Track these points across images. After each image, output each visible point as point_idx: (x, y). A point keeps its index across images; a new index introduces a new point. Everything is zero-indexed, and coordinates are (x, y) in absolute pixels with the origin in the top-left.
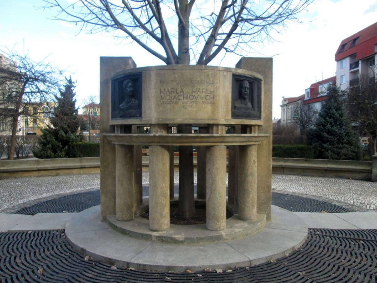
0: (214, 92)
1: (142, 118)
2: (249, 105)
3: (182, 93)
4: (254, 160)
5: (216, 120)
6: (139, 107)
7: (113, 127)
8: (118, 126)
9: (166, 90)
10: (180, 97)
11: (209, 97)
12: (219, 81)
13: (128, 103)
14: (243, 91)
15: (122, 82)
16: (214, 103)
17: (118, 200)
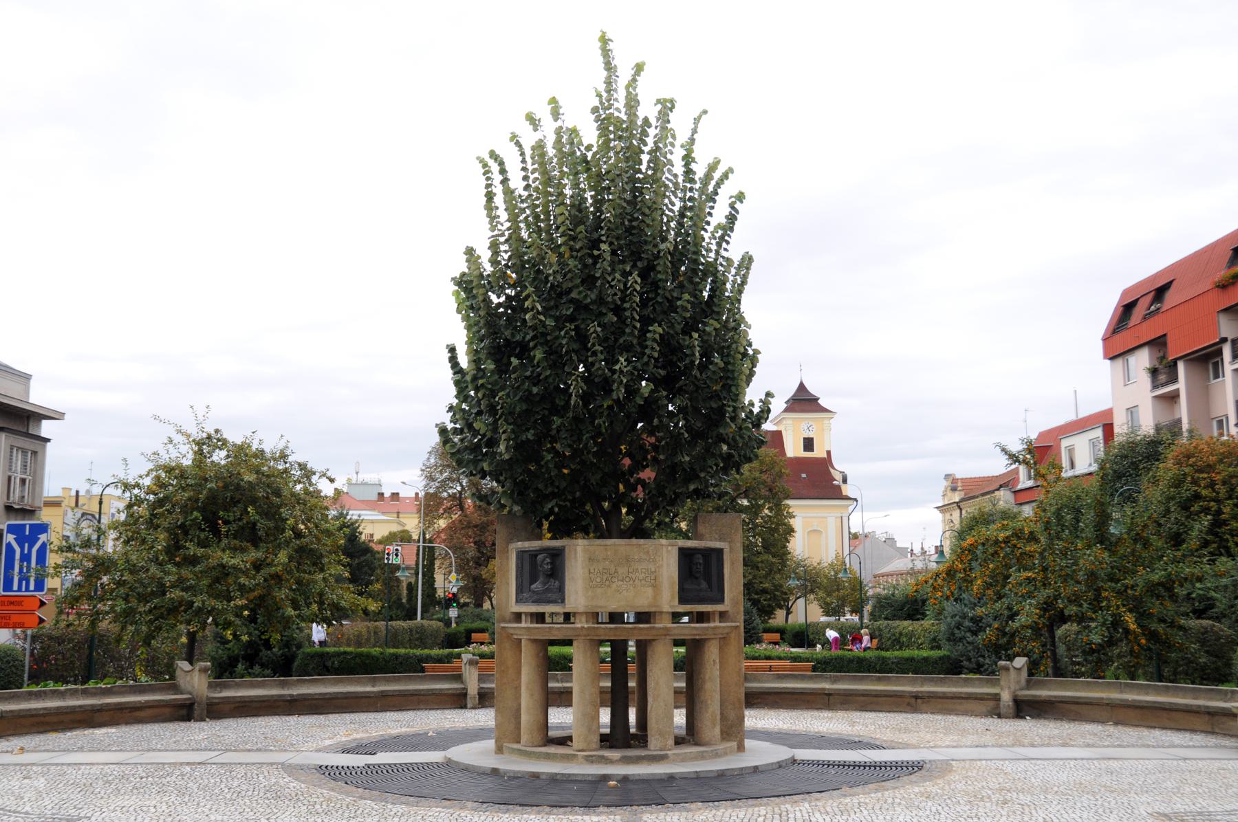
2: (704, 585)
6: (561, 589)
7: (518, 617)
8: (526, 614)
13: (545, 584)
15: (536, 556)
16: (655, 586)
17: (524, 718)
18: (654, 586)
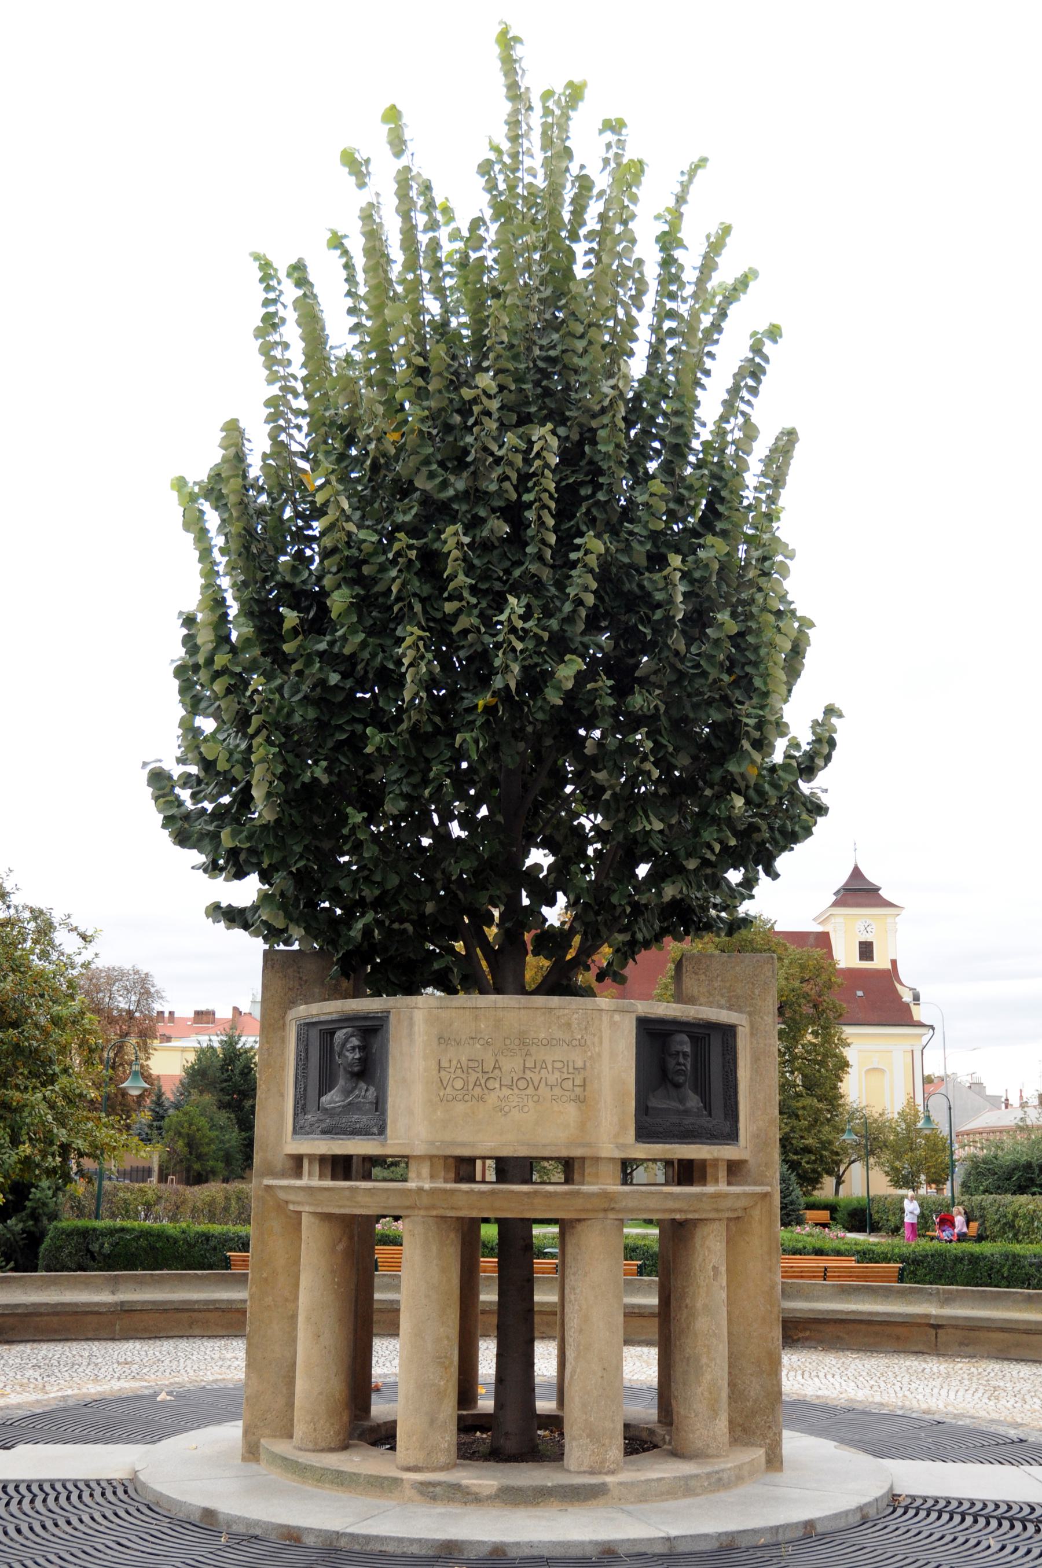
0: (584, 1068)
1: (386, 1139)
2: (693, 1101)
3: (497, 1071)
4: (714, 1267)
5: (588, 1145)
6: (379, 1106)
7: (297, 1162)
8: (311, 1157)
9: (454, 1062)
10: (491, 1084)
11: (570, 1082)
12: (601, 1038)
13: (347, 1093)
14: (671, 1063)
15: (332, 1033)
16: (583, 1101)
17: (301, 1385)
18: (581, 1100)
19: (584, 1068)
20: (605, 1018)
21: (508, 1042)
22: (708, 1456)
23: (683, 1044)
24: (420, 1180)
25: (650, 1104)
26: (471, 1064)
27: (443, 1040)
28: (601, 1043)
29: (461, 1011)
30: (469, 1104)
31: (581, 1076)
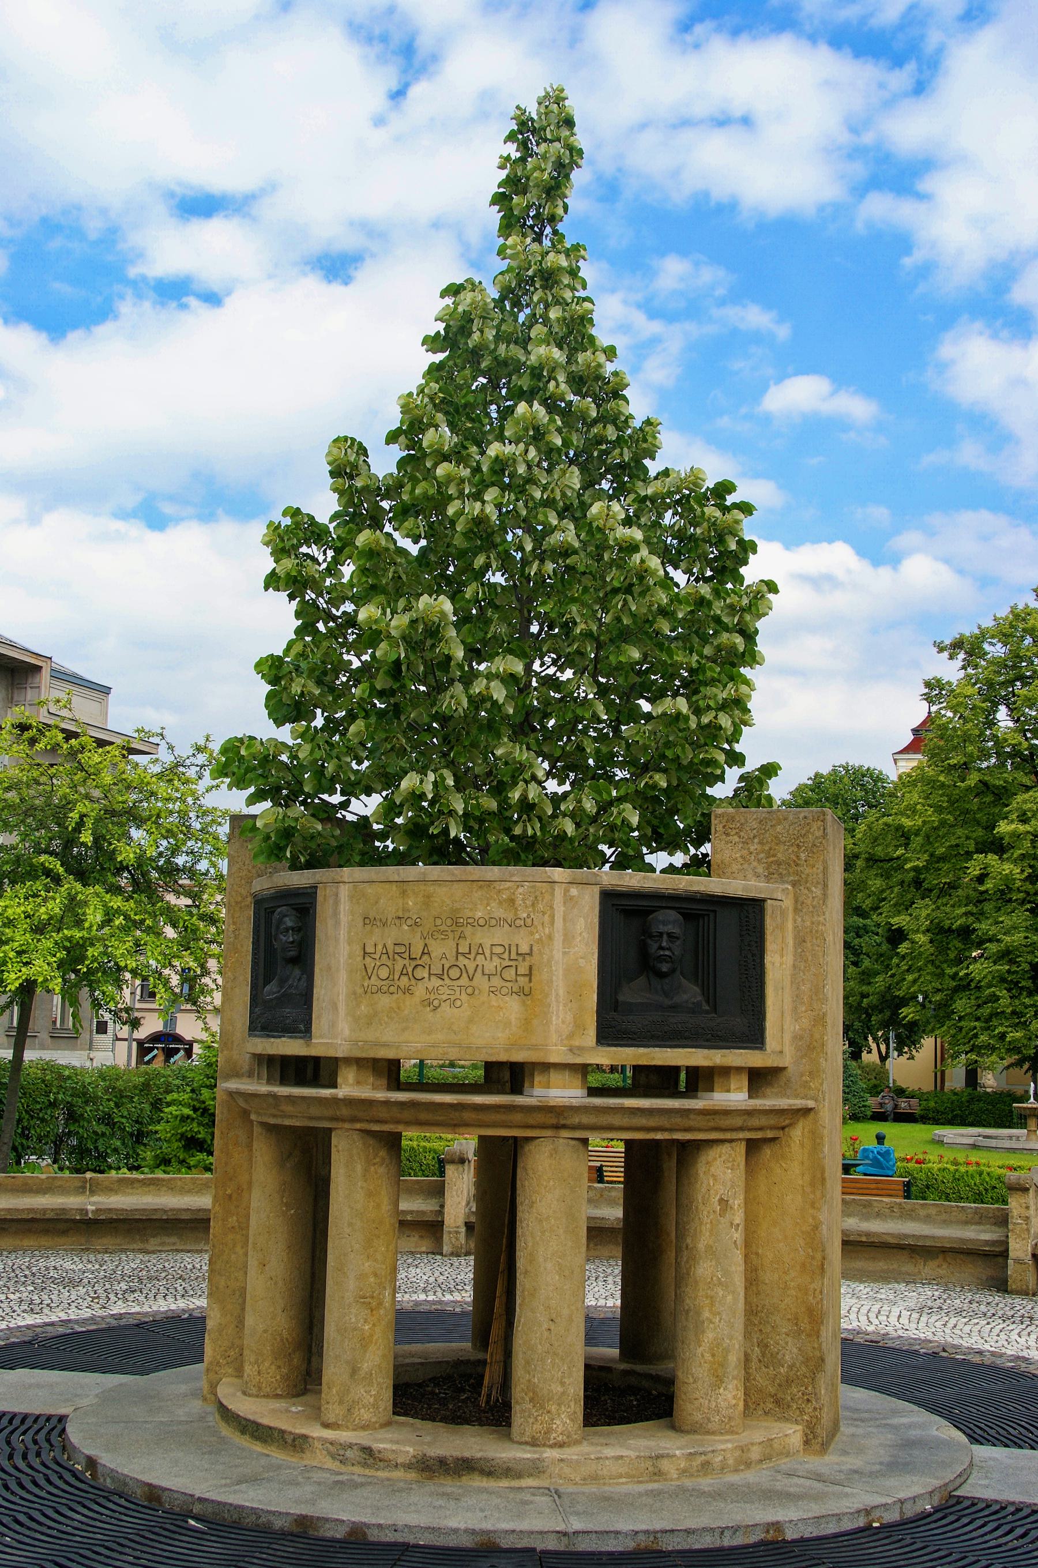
0: (530, 954)
1: (310, 1037)
2: (691, 993)
3: (426, 957)
4: (721, 1200)
5: (533, 1048)
9: (380, 947)
10: (420, 973)
11: (513, 971)
12: (552, 917)
14: (653, 946)
18: (525, 993)
19: (530, 954)
20: (559, 891)
21: (438, 922)
22: (682, 1431)
23: (668, 922)
24: (350, 1086)
25: (621, 998)
26: (398, 949)
27: (367, 920)
28: (552, 923)
29: (387, 886)
30: (395, 996)
31: (527, 964)
